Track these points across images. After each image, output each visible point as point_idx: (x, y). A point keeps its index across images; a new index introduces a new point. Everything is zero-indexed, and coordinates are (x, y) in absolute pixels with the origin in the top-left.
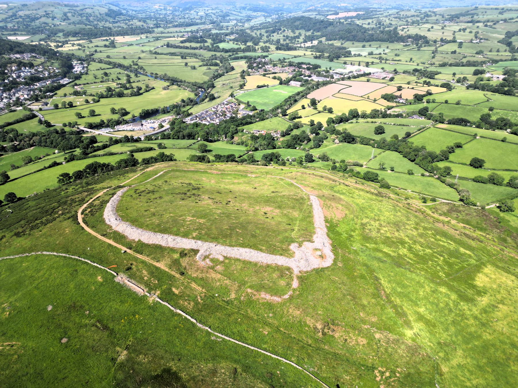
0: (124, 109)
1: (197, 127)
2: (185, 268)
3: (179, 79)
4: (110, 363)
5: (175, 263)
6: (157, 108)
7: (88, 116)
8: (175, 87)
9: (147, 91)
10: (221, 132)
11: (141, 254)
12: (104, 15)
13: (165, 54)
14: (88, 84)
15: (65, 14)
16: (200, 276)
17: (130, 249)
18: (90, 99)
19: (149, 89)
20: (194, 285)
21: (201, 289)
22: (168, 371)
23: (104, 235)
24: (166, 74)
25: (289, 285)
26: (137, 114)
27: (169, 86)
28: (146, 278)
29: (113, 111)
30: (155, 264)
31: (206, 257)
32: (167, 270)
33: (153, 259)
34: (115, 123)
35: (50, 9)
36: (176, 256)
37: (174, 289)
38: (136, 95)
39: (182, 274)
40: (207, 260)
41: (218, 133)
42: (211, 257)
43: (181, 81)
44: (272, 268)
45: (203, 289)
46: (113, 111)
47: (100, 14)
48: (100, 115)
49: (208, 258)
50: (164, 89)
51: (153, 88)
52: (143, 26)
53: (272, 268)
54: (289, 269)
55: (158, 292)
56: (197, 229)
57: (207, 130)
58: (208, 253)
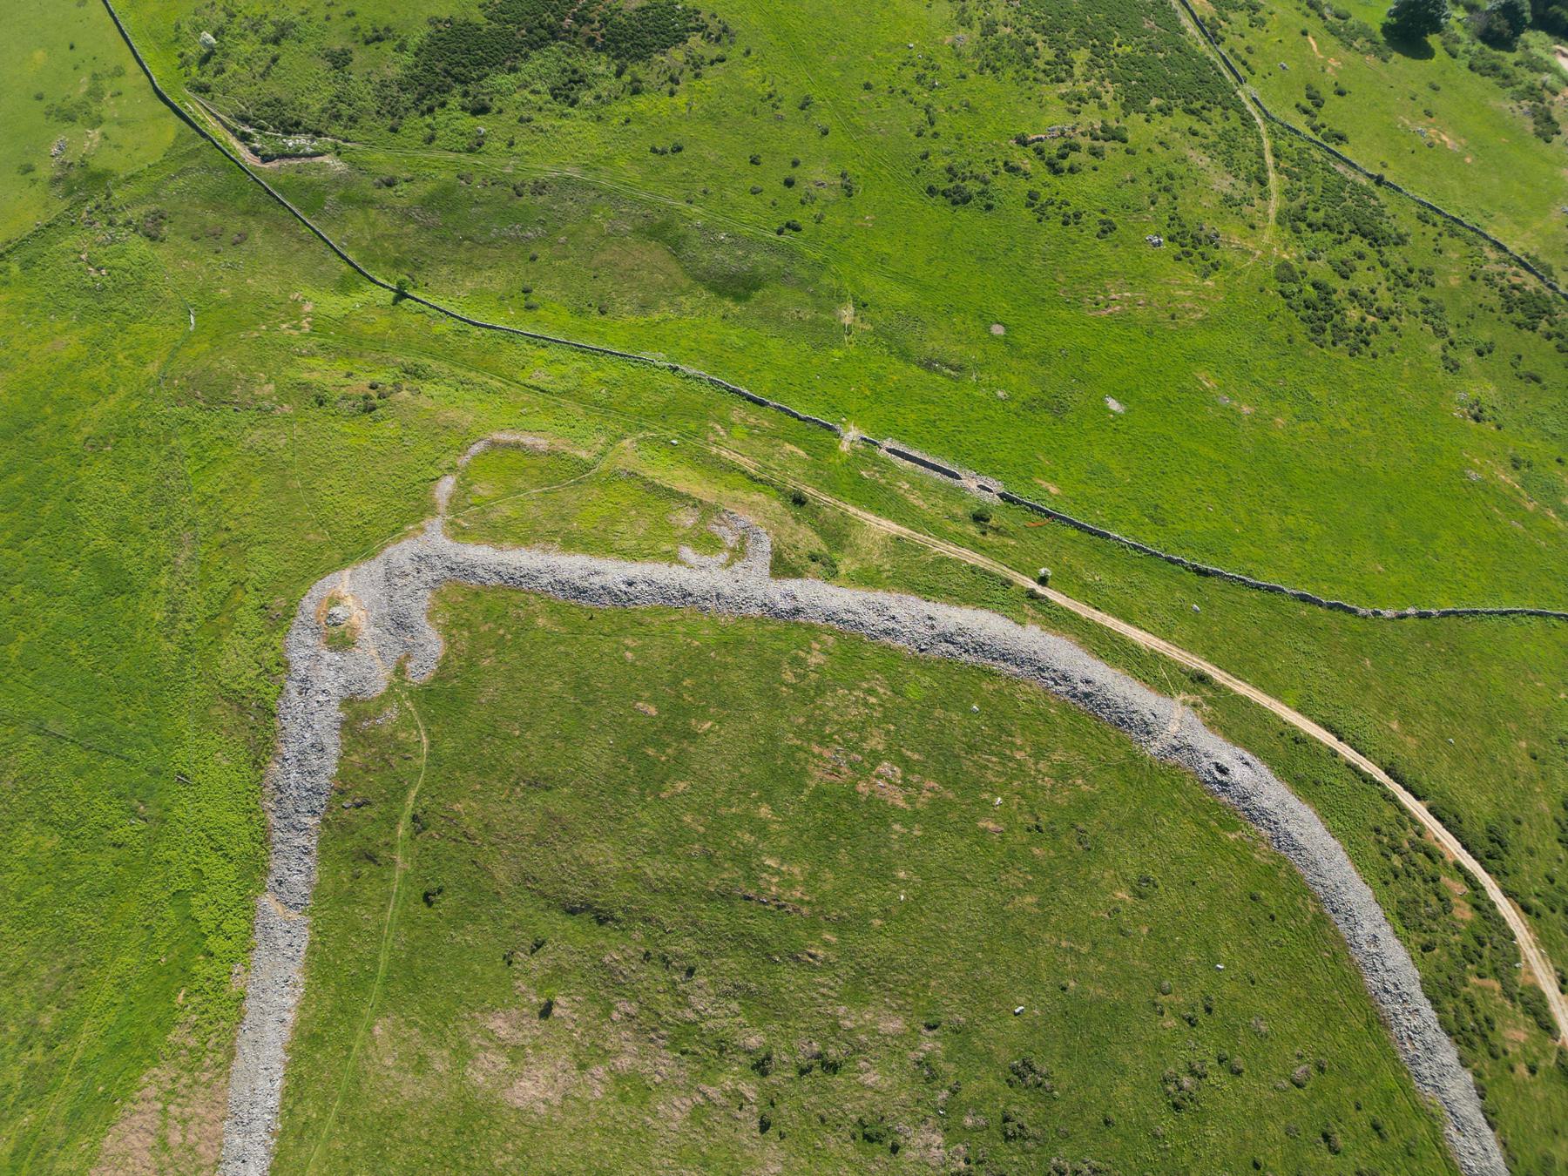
2: (797, 520)
4: (864, 298)
5: (837, 535)
11: (973, 569)
16: (740, 494)
17: (1032, 595)
20: (749, 464)
21: (724, 453)
22: (737, 298)
23: (1201, 679)
25: (464, 487)
28: (907, 486)
30: (905, 531)
31: (739, 553)
32: (852, 510)
33: (921, 549)
36: (846, 564)
37: (802, 453)
39: (799, 501)
40: (731, 540)
42: (723, 557)
44: (514, 534)
45: (718, 456)
49: (733, 550)
53: (514, 534)
54: (458, 533)
55: (845, 447)
56: (820, 690)
58: (738, 565)
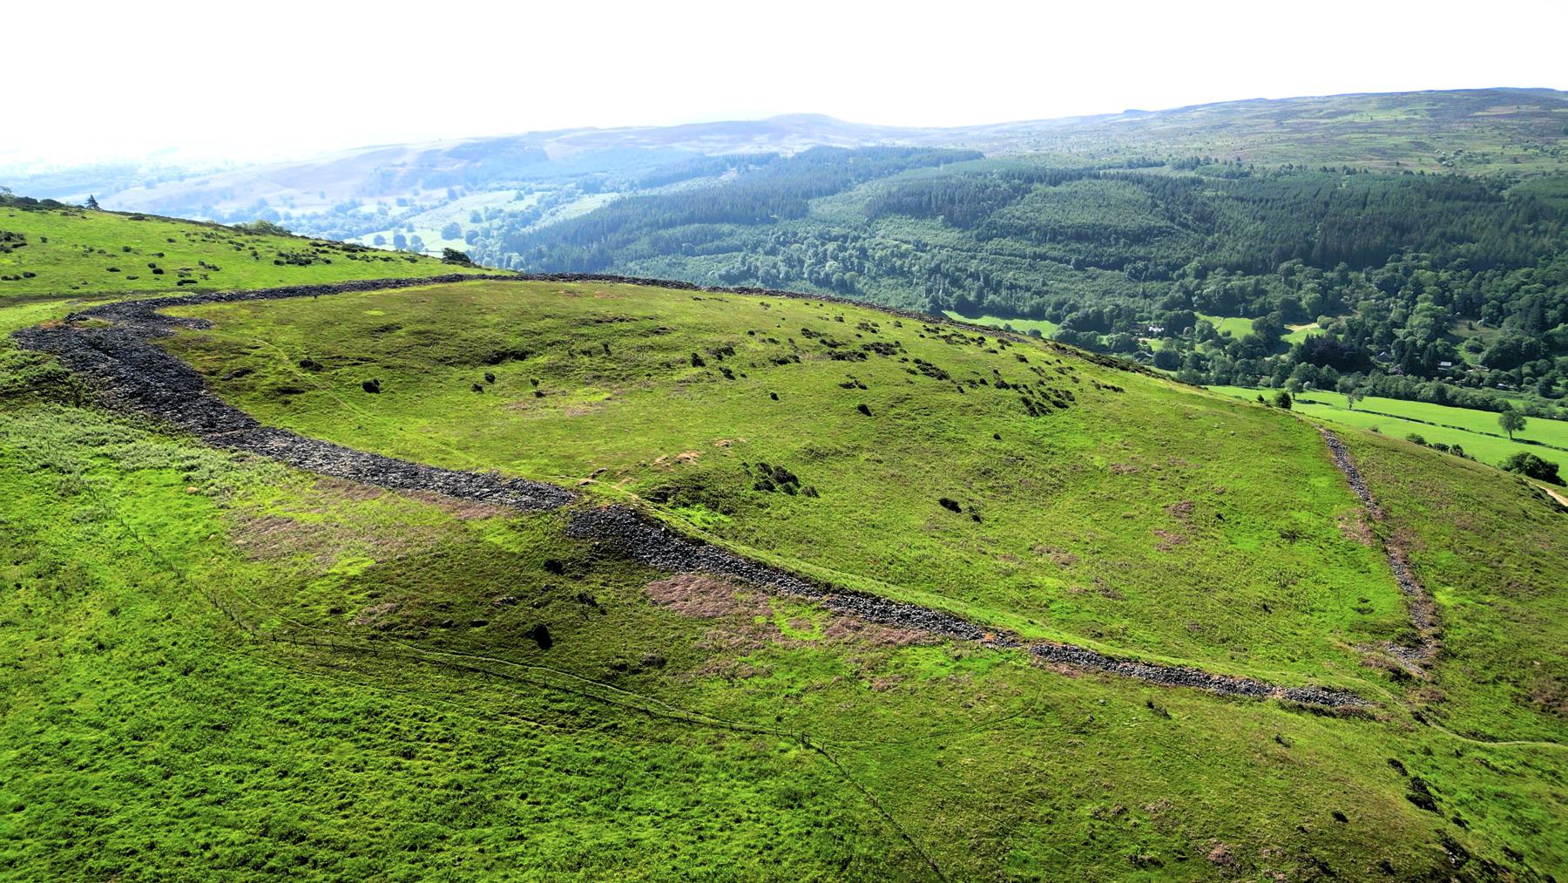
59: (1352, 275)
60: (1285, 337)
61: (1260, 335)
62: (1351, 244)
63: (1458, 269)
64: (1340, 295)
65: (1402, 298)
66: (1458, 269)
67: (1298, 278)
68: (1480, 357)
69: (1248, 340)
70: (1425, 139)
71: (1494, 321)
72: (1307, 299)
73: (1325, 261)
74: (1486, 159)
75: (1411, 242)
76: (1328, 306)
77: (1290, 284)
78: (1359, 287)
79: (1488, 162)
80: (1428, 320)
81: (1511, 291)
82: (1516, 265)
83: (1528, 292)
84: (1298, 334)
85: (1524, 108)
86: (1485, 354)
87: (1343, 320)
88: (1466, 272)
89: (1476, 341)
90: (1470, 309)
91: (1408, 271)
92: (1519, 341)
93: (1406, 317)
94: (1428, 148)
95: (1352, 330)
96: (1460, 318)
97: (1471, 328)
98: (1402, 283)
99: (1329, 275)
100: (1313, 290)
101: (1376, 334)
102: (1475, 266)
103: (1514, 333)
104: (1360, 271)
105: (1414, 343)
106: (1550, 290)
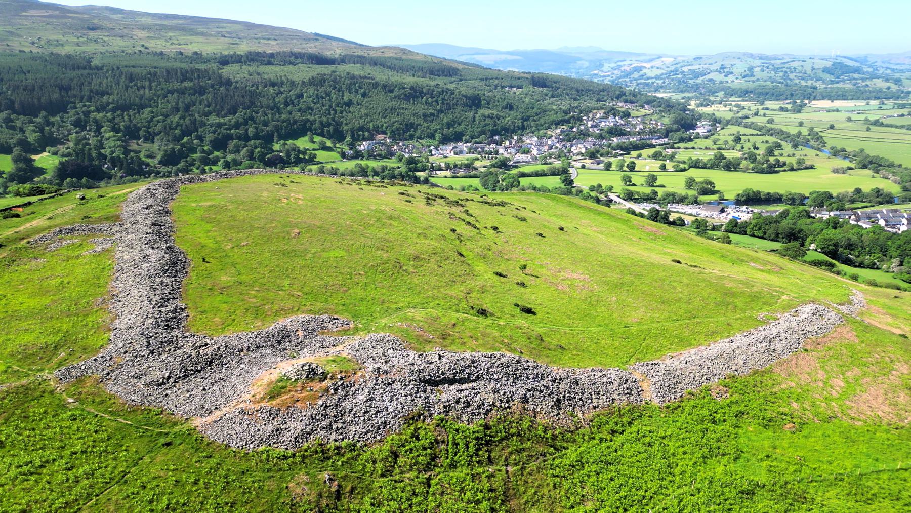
0: (711, 183)
1: (835, 228)
3: (887, 160)
6: (782, 192)
7: (642, 185)
8: (867, 172)
9: (792, 169)
10: (893, 251)
12: (820, 71)
13: (897, 127)
14: (693, 148)
15: (751, 69)
18: (669, 165)
19: (802, 166)
24: (862, 151)
26: (731, 196)
27: (851, 169)
29: (690, 183)
34: (671, 198)
35: (727, 63)
38: (762, 172)
41: (884, 251)
43: (891, 165)
46: (690, 183)
47: (813, 69)
48: (663, 187)
50: (836, 171)
51: (811, 167)
52: (889, 88)
57: (854, 238)
59: (52, 119)
60: (38, 164)
61: (21, 165)
62: (39, 99)
63: (114, 110)
64: (52, 133)
65: (90, 130)
66: (114, 110)
67: (18, 124)
68: (156, 161)
69: (19, 169)
70: (10, 29)
71: (150, 138)
72: (32, 137)
73: (30, 111)
74: (59, 44)
75: (75, 96)
76: (47, 142)
77: (13, 128)
78: (60, 126)
79: (62, 45)
80: (119, 143)
81: (149, 122)
82: (142, 107)
83: (158, 121)
84: (46, 160)
85: (50, 12)
86: (159, 157)
87: (62, 149)
88: (119, 112)
89: (152, 150)
90: (132, 133)
91: (87, 114)
92: (173, 149)
93: (100, 142)
94: (19, 36)
95: (79, 153)
96: (129, 139)
97: (138, 145)
98: (86, 122)
99: (38, 120)
100: (34, 131)
101: (94, 155)
102: (124, 108)
103: (166, 145)
104: (54, 115)
105: (119, 156)
106: (168, 120)
